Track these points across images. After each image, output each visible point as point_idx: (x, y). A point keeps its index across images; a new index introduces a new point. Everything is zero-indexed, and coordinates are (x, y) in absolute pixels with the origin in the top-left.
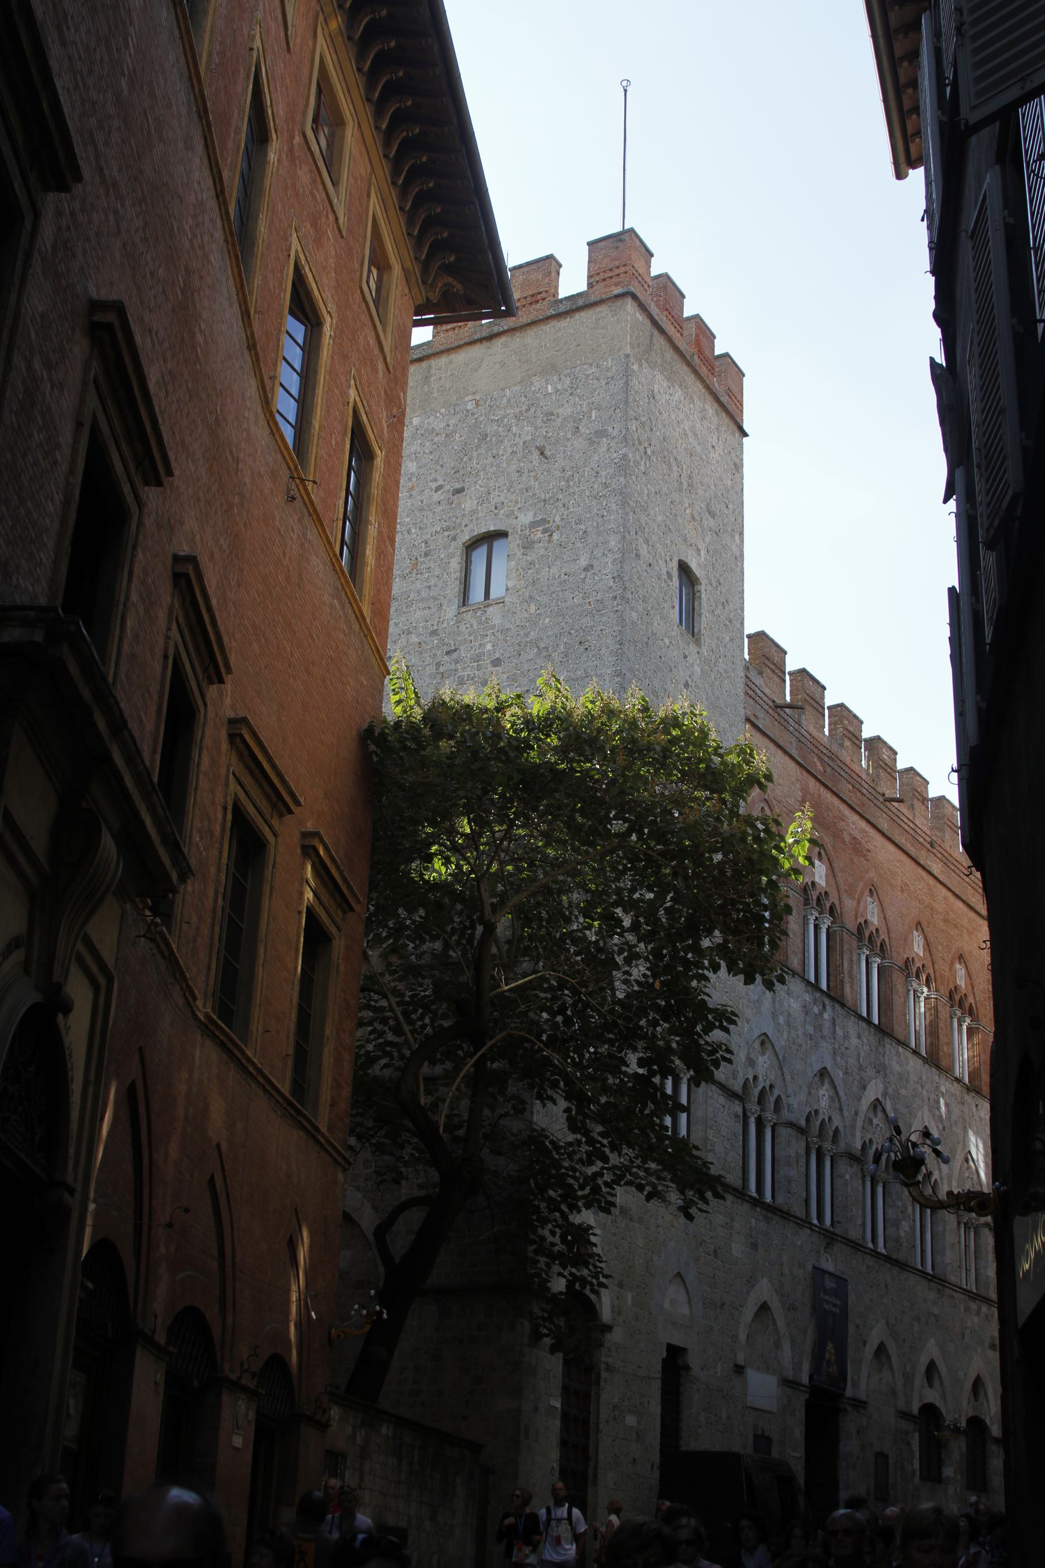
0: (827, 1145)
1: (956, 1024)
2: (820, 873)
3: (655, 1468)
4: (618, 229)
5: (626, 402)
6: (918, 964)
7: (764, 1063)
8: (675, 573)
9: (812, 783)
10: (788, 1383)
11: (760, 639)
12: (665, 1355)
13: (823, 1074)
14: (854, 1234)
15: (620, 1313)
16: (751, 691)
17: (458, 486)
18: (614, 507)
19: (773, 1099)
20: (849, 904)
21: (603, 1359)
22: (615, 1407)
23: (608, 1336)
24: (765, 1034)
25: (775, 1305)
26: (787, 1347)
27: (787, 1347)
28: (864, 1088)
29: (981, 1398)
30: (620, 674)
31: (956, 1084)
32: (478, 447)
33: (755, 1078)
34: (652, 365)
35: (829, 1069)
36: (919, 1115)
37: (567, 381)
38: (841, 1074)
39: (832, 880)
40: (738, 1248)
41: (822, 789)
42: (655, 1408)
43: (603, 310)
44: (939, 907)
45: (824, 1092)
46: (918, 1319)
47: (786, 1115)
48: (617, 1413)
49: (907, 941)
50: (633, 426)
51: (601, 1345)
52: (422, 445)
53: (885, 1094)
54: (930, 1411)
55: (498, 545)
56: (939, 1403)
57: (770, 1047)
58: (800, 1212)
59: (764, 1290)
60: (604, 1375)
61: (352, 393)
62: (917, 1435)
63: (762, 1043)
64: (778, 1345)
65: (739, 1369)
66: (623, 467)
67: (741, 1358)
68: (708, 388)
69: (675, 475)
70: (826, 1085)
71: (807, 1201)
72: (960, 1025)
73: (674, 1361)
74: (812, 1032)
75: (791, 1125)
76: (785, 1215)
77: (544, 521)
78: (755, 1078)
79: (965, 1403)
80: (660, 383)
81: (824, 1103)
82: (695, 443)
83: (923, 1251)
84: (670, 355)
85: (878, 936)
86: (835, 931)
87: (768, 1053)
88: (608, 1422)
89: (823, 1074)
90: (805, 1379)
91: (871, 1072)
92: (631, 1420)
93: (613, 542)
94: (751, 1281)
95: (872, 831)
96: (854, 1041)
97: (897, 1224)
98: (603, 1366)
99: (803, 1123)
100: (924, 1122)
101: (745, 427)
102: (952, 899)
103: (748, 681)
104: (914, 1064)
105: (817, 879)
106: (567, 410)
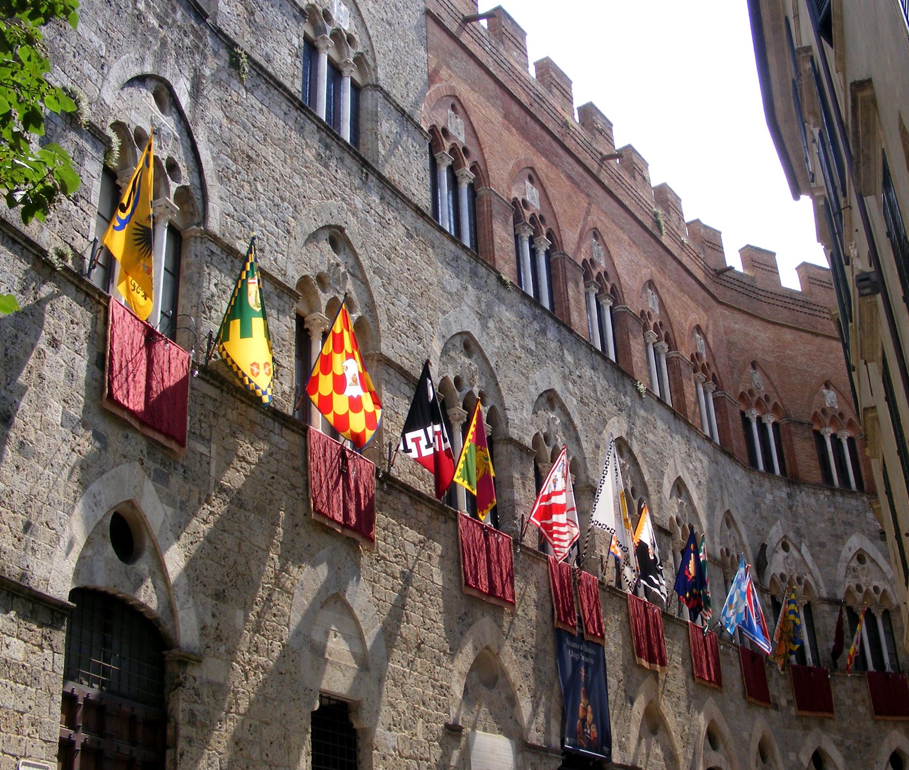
1: (701, 389)
6: (655, 319)
15: (219, 638)
21: (182, 705)
23: (193, 671)
24: (468, 333)
28: (605, 422)
29: (769, 760)
31: (708, 444)
35: (559, 392)
36: (671, 462)
38: (575, 402)
41: (529, 119)
51: (180, 684)
53: (630, 433)
57: (478, 351)
65: (453, 731)
70: (557, 410)
72: (705, 393)
74: (533, 348)
75: (511, 440)
85: (608, 279)
86: (556, 259)
87: (475, 357)
90: (555, 742)
91: (610, 407)
95: (590, 179)
98: (181, 717)
99: (528, 441)
100: (677, 472)
102: (684, 274)
105: (528, 199)
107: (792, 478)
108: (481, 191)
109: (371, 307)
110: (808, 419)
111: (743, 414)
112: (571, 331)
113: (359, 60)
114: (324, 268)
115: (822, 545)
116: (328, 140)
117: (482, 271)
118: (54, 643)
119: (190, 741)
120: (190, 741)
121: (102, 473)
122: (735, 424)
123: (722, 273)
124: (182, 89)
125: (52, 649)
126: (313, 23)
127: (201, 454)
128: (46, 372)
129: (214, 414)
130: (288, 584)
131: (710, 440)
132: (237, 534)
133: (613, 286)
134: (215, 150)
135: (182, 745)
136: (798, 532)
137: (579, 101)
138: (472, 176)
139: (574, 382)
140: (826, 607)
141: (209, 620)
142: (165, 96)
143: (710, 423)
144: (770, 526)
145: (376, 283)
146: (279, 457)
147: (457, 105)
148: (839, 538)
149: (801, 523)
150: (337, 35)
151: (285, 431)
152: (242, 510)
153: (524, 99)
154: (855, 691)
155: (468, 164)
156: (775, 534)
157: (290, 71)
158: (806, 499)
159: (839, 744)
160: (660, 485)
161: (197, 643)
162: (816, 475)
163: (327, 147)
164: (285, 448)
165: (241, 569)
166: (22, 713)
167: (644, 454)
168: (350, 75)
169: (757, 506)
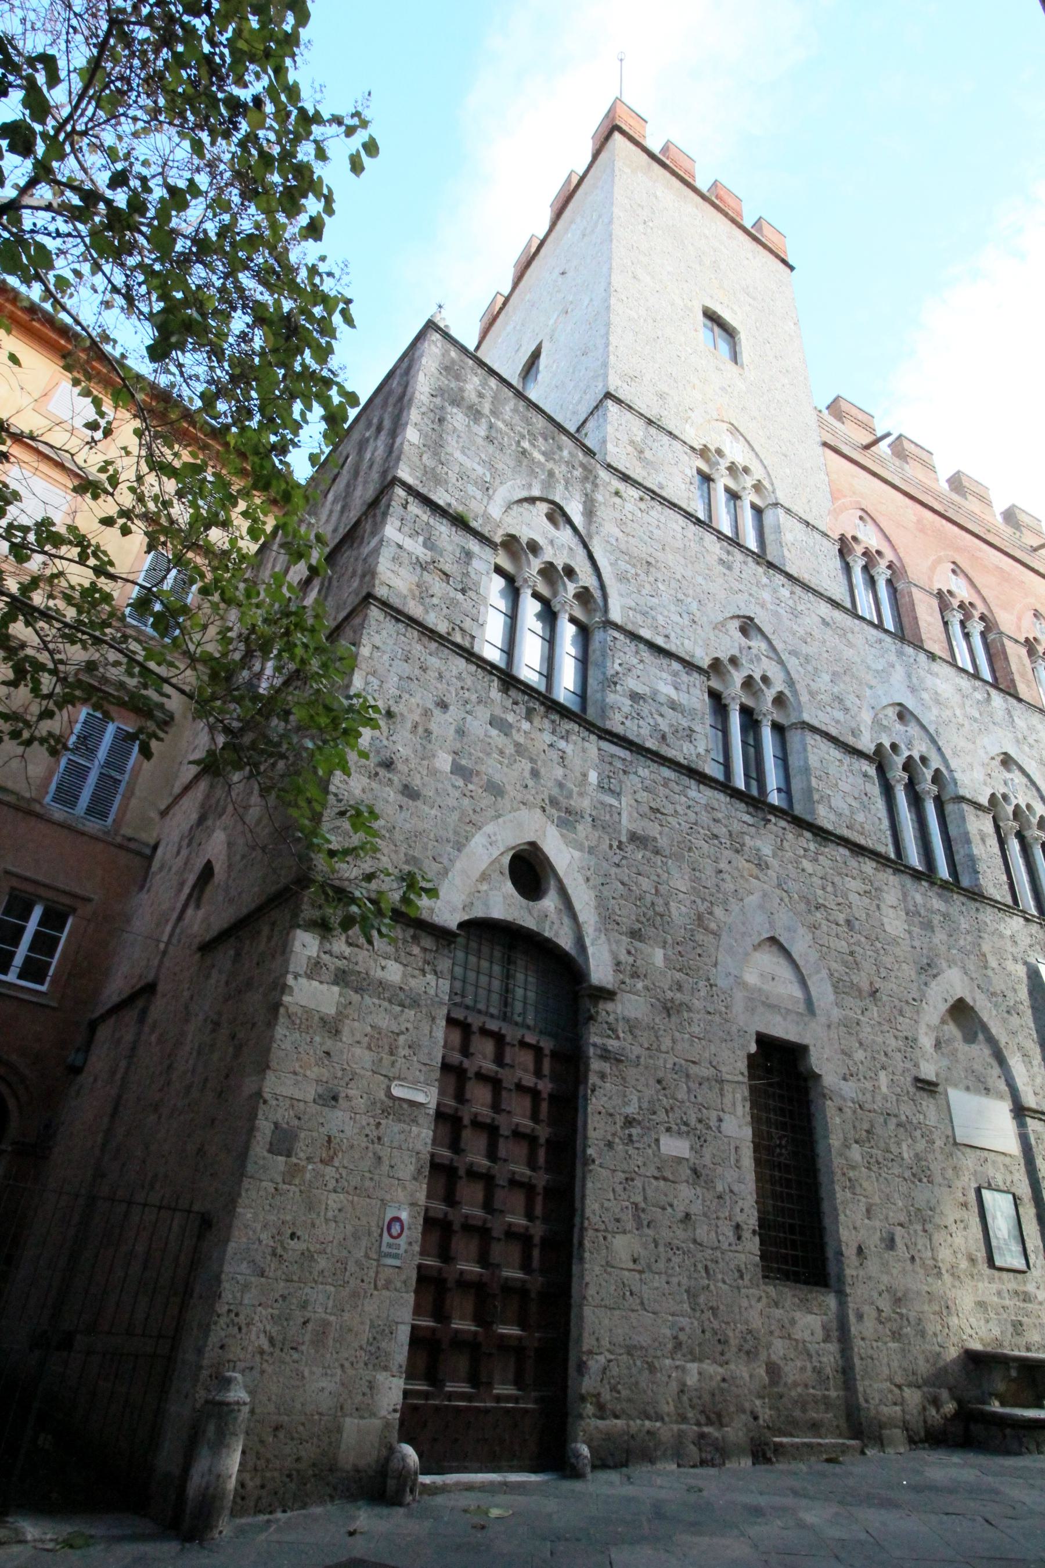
3: (747, 1234)
12: (753, 1048)
15: (635, 975)
21: (595, 1039)
22: (629, 1122)
23: (610, 1006)
39: (972, 591)
40: (894, 924)
48: (634, 1131)
60: (595, 1065)
67: (928, 1071)
74: (977, 716)
88: (610, 1145)
92: (675, 1146)
94: (928, 969)
99: (984, 801)
101: (791, 263)
108: (900, 586)
109: (791, 683)
112: (1020, 700)
113: (758, 487)
114: (735, 652)
116: (730, 548)
117: (909, 650)
118: (439, 969)
119: (603, 1076)
120: (603, 1076)
121: (499, 816)
124: (575, 510)
125: (436, 973)
126: (707, 460)
127: (611, 806)
128: (433, 727)
129: (625, 772)
130: (713, 926)
132: (656, 878)
134: (613, 558)
135: (593, 1079)
137: (1000, 506)
138: (889, 572)
139: (1031, 746)
141: (623, 957)
142: (557, 515)
145: (792, 663)
146: (697, 809)
150: (732, 469)
151: (702, 787)
152: (659, 857)
155: (883, 563)
157: (685, 495)
161: (611, 978)
163: (728, 553)
164: (703, 801)
165: (660, 909)
166: (398, 1034)
168: (749, 497)
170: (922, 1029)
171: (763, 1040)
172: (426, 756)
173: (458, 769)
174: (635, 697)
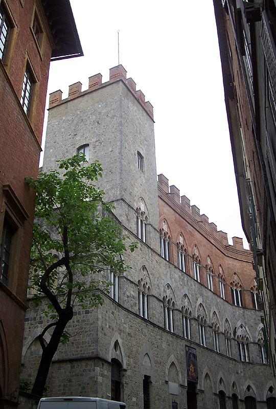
0: (188, 316)
2: (181, 240)
4: (118, 65)
5: (121, 107)
6: (209, 266)
7: (168, 292)
8: (137, 154)
9: (177, 215)
10: (181, 386)
11: (161, 176)
13: (186, 295)
14: (197, 342)
16: (160, 189)
17: (75, 133)
18: (118, 134)
19: (172, 302)
20: (190, 249)
21: (124, 380)
25: (176, 363)
26: (180, 375)
27: (180, 375)
30: (121, 178)
32: (80, 123)
33: (166, 296)
34: (128, 99)
37: (105, 103)
40: (164, 345)
42: (142, 395)
43: (114, 85)
44: (214, 251)
45: (186, 300)
46: (216, 365)
47: (176, 307)
49: (206, 261)
50: (123, 114)
52: (66, 124)
53: (203, 302)
54: (222, 393)
55: (87, 149)
56: (224, 390)
58: (181, 335)
59: (172, 358)
60: (125, 385)
61: (27, 57)
62: (219, 400)
63: (168, 286)
64: (178, 375)
65: (167, 382)
66: (121, 124)
68: (143, 108)
69: (135, 129)
71: (183, 332)
73: (147, 381)
75: (177, 310)
76: (178, 336)
77: (99, 140)
78: (166, 296)
79: (231, 390)
80: (130, 105)
81: (186, 304)
82: (140, 121)
83: (216, 346)
84: (132, 98)
89: (186, 295)
90: (186, 385)
91: (198, 295)
92: (134, 399)
93: (118, 143)
94: (169, 356)
96: (193, 286)
97: (209, 338)
99: (181, 309)
103: (159, 187)
104: (210, 294)
106: (104, 111)
107: (244, 307)
109: (151, 283)
110: (250, 290)
111: (231, 288)
115: (252, 326)
120: (125, 387)
122: (229, 292)
123: (228, 247)
131: (222, 299)
133: (200, 260)
136: (245, 323)
140: (252, 345)
143: (223, 295)
144: (238, 321)
147: (165, 220)
148: (257, 324)
149: (246, 320)
153: (179, 211)
154: (260, 369)
156: (239, 324)
158: (248, 313)
159: (254, 384)
160: (210, 314)
162: (251, 306)
167: (206, 307)
169: (235, 315)
170: (166, 369)
171: (145, 376)
172: (106, 325)
173: (110, 327)
174: (128, 297)
